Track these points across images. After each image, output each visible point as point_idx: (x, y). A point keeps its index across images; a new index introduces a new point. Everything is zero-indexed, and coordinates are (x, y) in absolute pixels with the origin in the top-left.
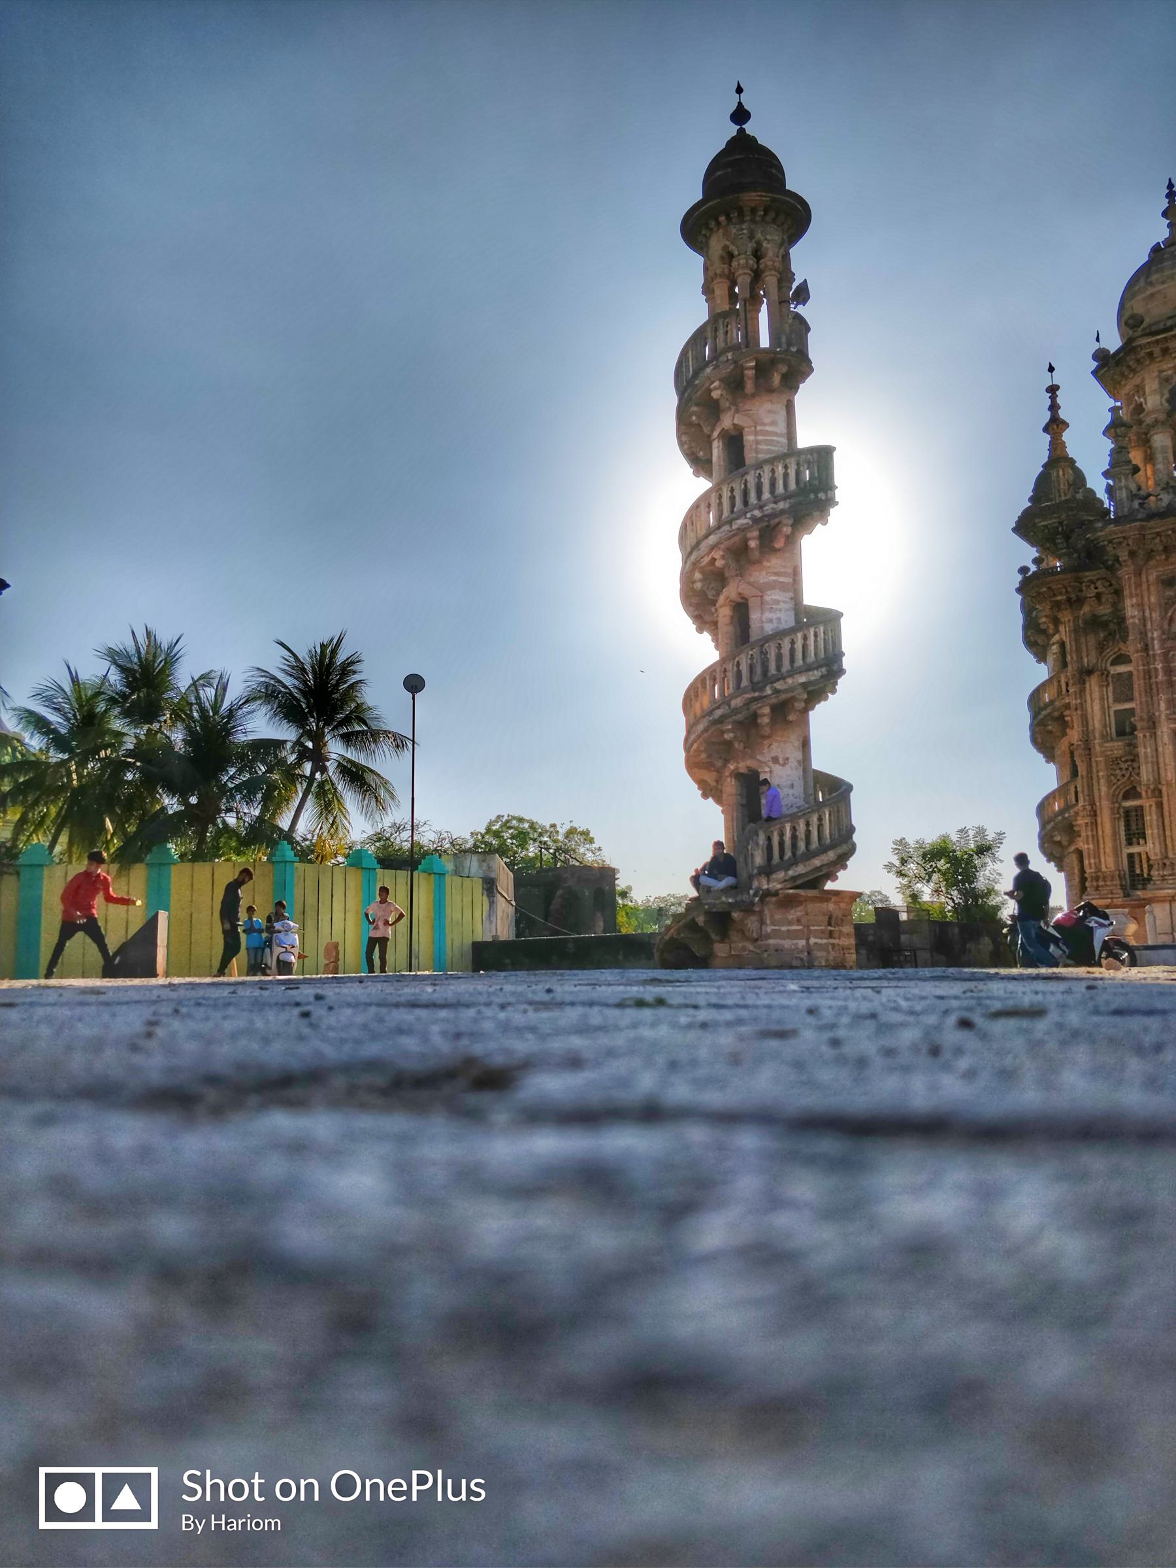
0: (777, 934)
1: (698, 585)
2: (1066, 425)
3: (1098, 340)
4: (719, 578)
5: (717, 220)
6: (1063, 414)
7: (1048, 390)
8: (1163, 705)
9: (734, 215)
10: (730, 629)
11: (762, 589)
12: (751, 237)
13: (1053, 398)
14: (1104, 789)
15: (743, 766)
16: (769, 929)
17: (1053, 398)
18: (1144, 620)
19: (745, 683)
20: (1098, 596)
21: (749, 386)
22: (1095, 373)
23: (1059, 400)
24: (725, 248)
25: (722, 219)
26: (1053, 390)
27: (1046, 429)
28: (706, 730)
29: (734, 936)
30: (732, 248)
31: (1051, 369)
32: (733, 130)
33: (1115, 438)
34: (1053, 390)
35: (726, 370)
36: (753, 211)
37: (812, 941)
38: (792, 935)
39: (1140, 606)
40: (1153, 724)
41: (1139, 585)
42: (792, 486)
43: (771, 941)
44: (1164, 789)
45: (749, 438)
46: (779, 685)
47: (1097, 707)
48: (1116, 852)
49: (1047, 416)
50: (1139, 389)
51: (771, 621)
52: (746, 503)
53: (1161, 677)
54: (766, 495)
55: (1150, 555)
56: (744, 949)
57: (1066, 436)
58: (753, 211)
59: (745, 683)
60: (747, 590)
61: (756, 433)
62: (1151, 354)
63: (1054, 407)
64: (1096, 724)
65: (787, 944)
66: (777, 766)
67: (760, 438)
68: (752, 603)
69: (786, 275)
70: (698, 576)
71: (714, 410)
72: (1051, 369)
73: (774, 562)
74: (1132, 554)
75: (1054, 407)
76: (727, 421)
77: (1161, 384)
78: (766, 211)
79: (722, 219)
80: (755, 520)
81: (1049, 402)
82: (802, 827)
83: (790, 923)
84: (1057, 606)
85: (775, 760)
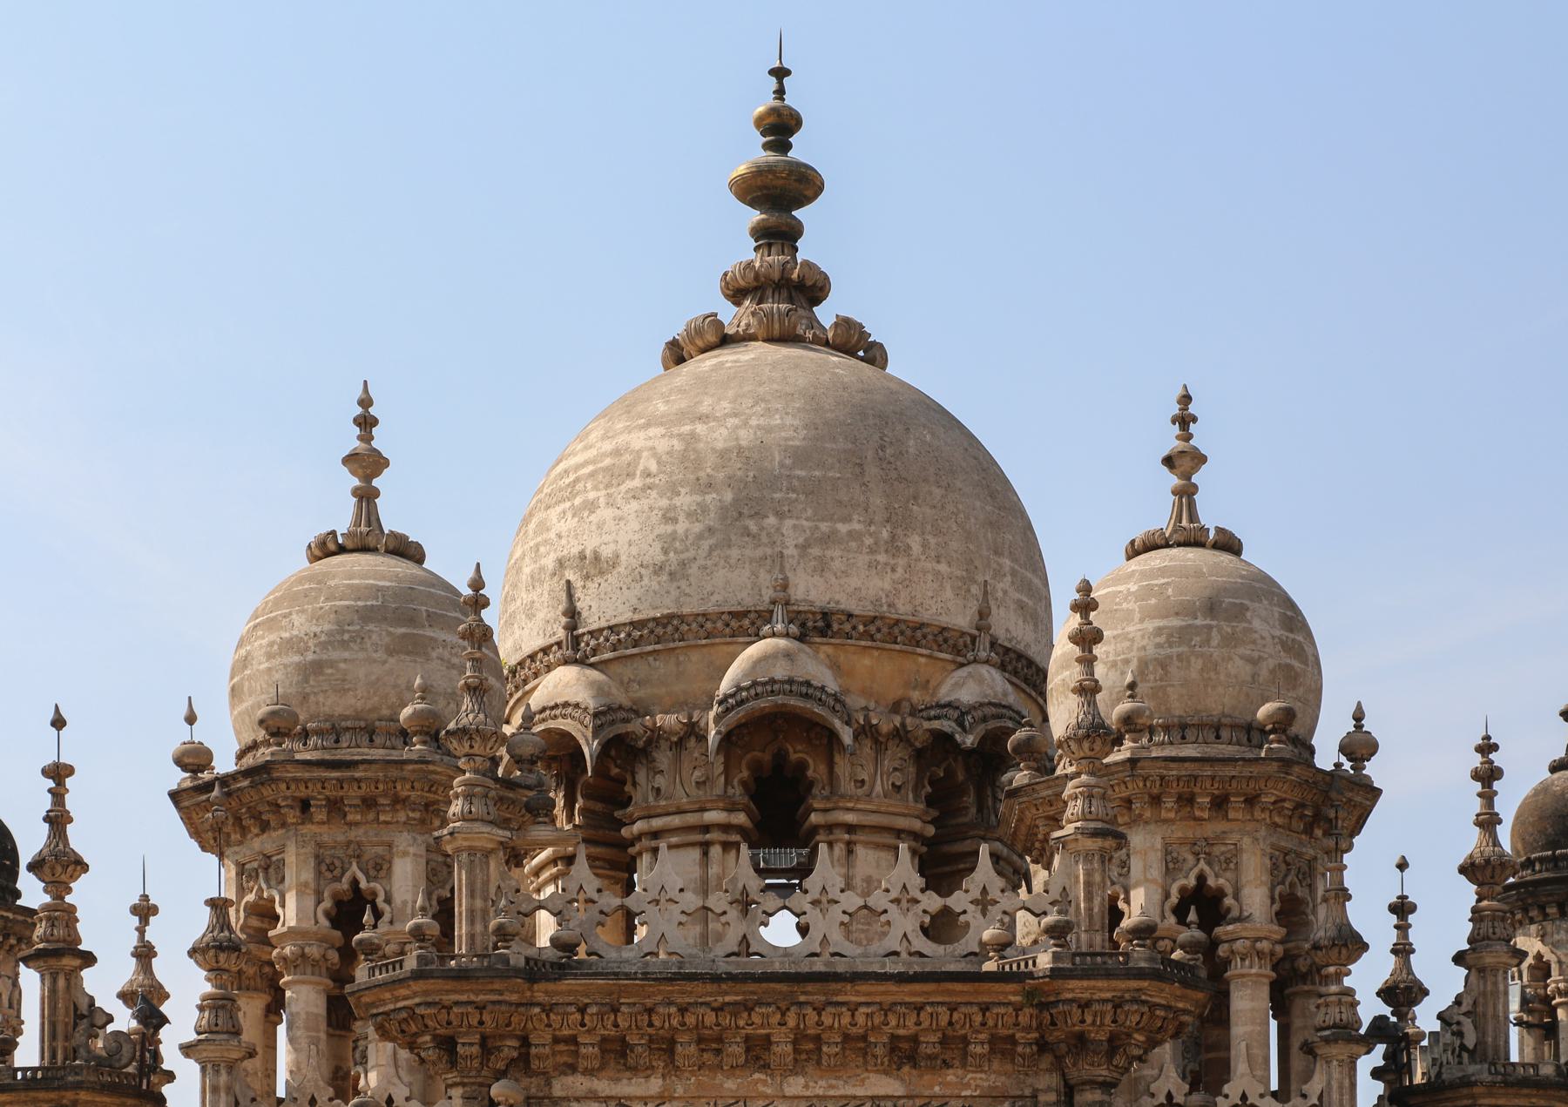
2: (80, 866)
3: (191, 719)
6: (77, 837)
7: (46, 772)
13: (58, 795)
17: (58, 795)
22: (175, 796)
23: (70, 803)
26: (58, 773)
31: (59, 723)
33: (215, 971)
34: (58, 773)
50: (270, 868)
62: (305, 805)
63: (58, 820)
72: (59, 723)
75: (58, 820)
77: (319, 873)
81: (46, 802)
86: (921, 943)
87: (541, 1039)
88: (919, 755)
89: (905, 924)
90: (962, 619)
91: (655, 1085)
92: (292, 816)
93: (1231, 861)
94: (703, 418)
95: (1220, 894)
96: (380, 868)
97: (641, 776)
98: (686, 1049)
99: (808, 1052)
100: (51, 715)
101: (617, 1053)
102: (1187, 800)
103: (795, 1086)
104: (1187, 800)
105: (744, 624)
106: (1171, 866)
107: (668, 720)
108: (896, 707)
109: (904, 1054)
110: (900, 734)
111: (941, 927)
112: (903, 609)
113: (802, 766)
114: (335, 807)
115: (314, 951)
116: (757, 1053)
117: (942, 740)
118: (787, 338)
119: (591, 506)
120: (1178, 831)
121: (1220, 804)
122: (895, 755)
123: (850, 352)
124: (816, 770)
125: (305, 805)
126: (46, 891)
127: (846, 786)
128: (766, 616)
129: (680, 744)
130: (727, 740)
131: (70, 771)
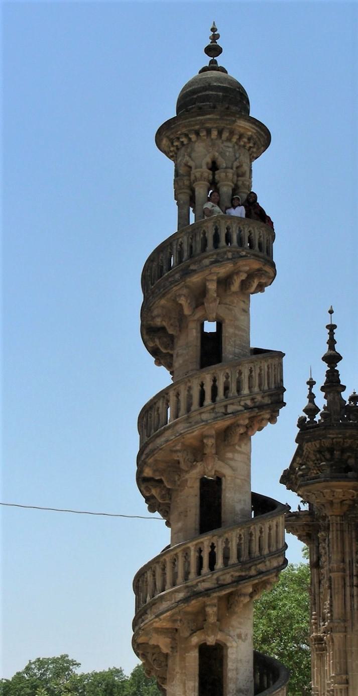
4: (198, 453)
5: (209, 132)
6: (338, 348)
9: (225, 135)
13: (332, 334)
15: (211, 640)
17: (332, 334)
19: (233, 560)
21: (236, 286)
23: (335, 337)
25: (214, 133)
26: (332, 328)
27: (325, 359)
28: (186, 600)
31: (331, 312)
32: (206, 60)
34: (332, 328)
36: (241, 136)
42: (273, 386)
46: (261, 567)
49: (325, 349)
52: (239, 390)
54: (256, 389)
57: (340, 367)
58: (241, 136)
59: (233, 560)
63: (332, 342)
66: (240, 641)
67: (237, 332)
73: (243, 448)
75: (332, 342)
78: (249, 139)
79: (214, 133)
80: (246, 407)
100: (329, 309)
126: (328, 366)
131: (334, 327)
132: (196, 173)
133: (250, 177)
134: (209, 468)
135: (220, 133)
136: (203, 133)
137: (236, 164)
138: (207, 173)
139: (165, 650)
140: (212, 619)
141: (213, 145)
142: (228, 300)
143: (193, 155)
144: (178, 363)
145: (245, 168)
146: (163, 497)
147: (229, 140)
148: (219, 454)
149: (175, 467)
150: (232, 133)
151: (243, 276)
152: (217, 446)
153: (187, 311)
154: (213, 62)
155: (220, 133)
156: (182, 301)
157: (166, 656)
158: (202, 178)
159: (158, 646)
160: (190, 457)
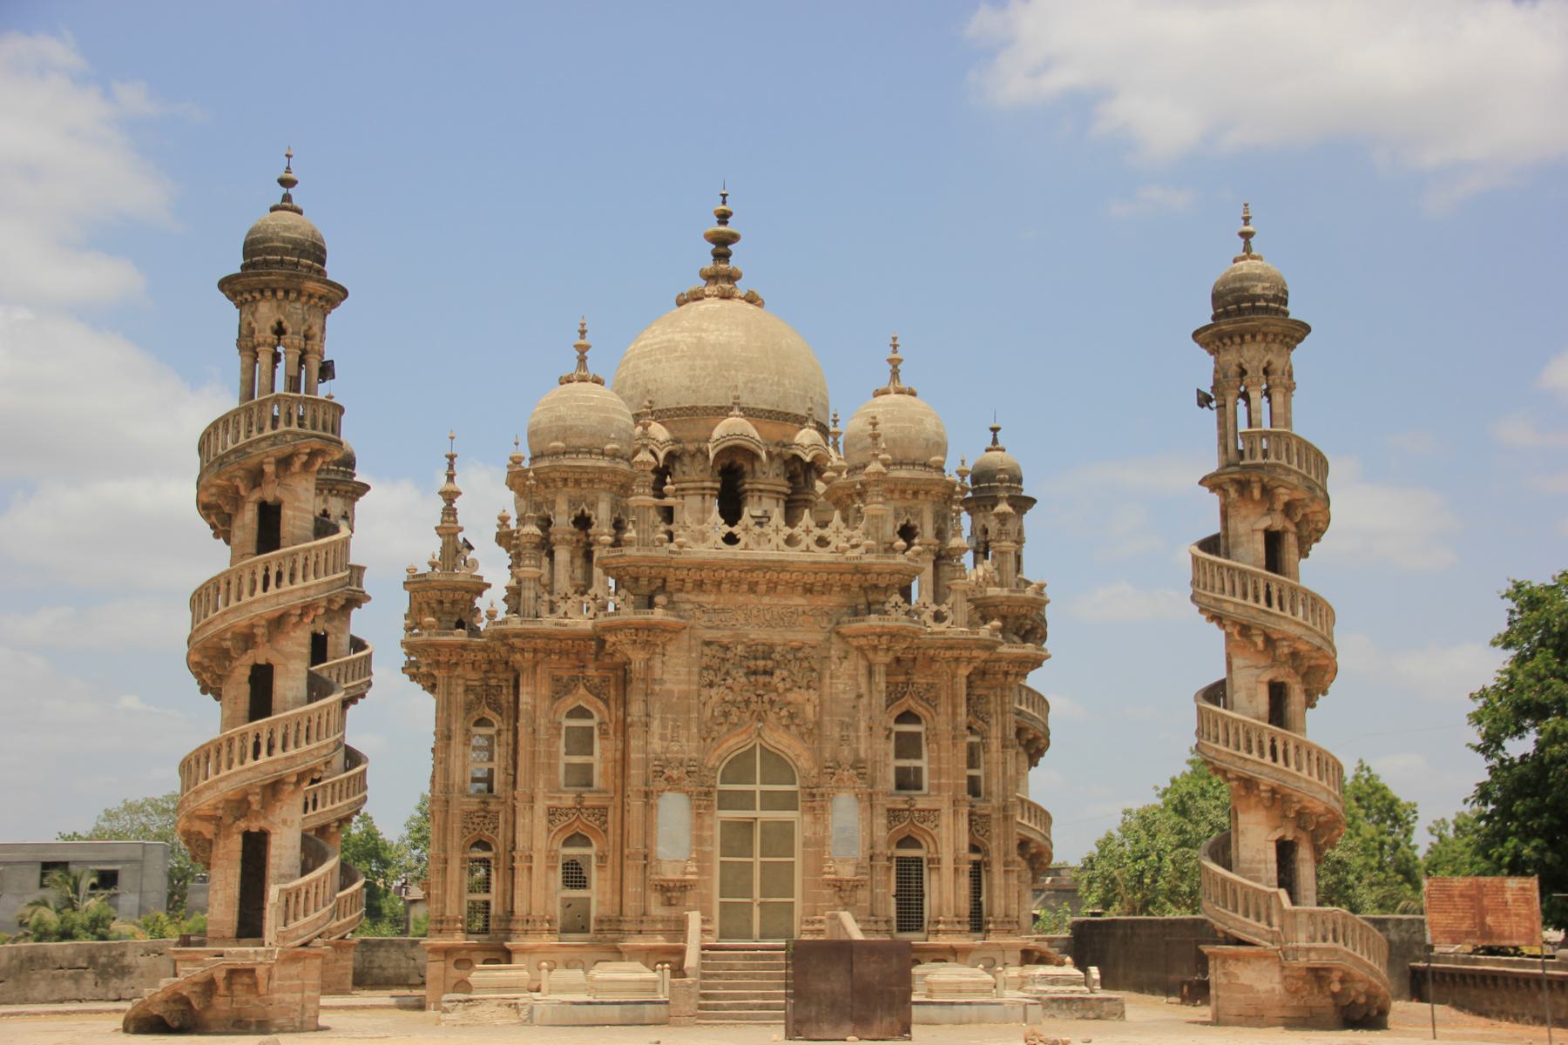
0: (280, 989)
1: (228, 644)
5: (274, 292)
8: (541, 784)
9: (293, 295)
10: (246, 689)
11: (288, 657)
12: (304, 320)
13: (451, 466)
14: (457, 839)
15: (254, 828)
16: (275, 984)
17: (451, 466)
18: (534, 707)
20: (473, 663)
21: (297, 465)
24: (280, 323)
25: (280, 294)
26: (451, 458)
29: (238, 989)
30: (285, 324)
34: (451, 458)
35: (288, 450)
36: (311, 296)
37: (307, 993)
38: (292, 990)
39: (534, 695)
40: (532, 799)
41: (535, 673)
43: (276, 996)
44: (535, 857)
45: (287, 513)
47: (459, 764)
48: (461, 897)
51: (291, 689)
53: (543, 760)
55: (549, 652)
56: (247, 1002)
60: (274, 658)
61: (295, 509)
64: (457, 777)
65: (288, 997)
68: (277, 671)
69: (322, 356)
70: (229, 635)
71: (256, 477)
74: (535, 651)
76: (270, 493)
79: (280, 294)
82: (313, 891)
83: (291, 978)
84: (438, 664)
85: (284, 822)
86: (813, 547)
87: (671, 579)
88: (785, 462)
89: (809, 540)
90: (803, 413)
91: (712, 598)
92: (560, 484)
93: (919, 514)
94: (706, 331)
95: (914, 528)
96: (593, 505)
97: (677, 466)
98: (725, 586)
99: (772, 588)
101: (700, 585)
102: (903, 492)
103: (766, 600)
104: (903, 492)
105: (722, 411)
106: (897, 517)
107: (691, 447)
108: (777, 444)
109: (808, 590)
110: (780, 455)
111: (822, 542)
112: (782, 409)
113: (741, 467)
114: (577, 482)
115: (568, 537)
116: (753, 588)
117: (796, 458)
118: (726, 296)
119: (659, 361)
120: (899, 504)
121: (915, 494)
122: (777, 463)
123: (751, 302)
124: (747, 467)
125: (565, 480)
127: (759, 474)
128: (731, 409)
129: (693, 456)
130: (717, 456)
132: (259, 337)
133: (322, 341)
134: (261, 655)
135: (287, 292)
136: (268, 294)
137: (304, 328)
138: (272, 338)
139: (209, 836)
140: (256, 807)
141: (279, 306)
142: (288, 481)
143: (257, 315)
144: (235, 540)
145: (316, 330)
146: (214, 682)
147: (297, 299)
148: (270, 638)
149: (225, 655)
150: (300, 293)
151: (304, 458)
152: (270, 633)
153: (243, 493)
154: (287, 198)
155: (287, 292)
156: (238, 482)
157: (210, 842)
158: (264, 343)
159: (200, 833)
160: (241, 644)
